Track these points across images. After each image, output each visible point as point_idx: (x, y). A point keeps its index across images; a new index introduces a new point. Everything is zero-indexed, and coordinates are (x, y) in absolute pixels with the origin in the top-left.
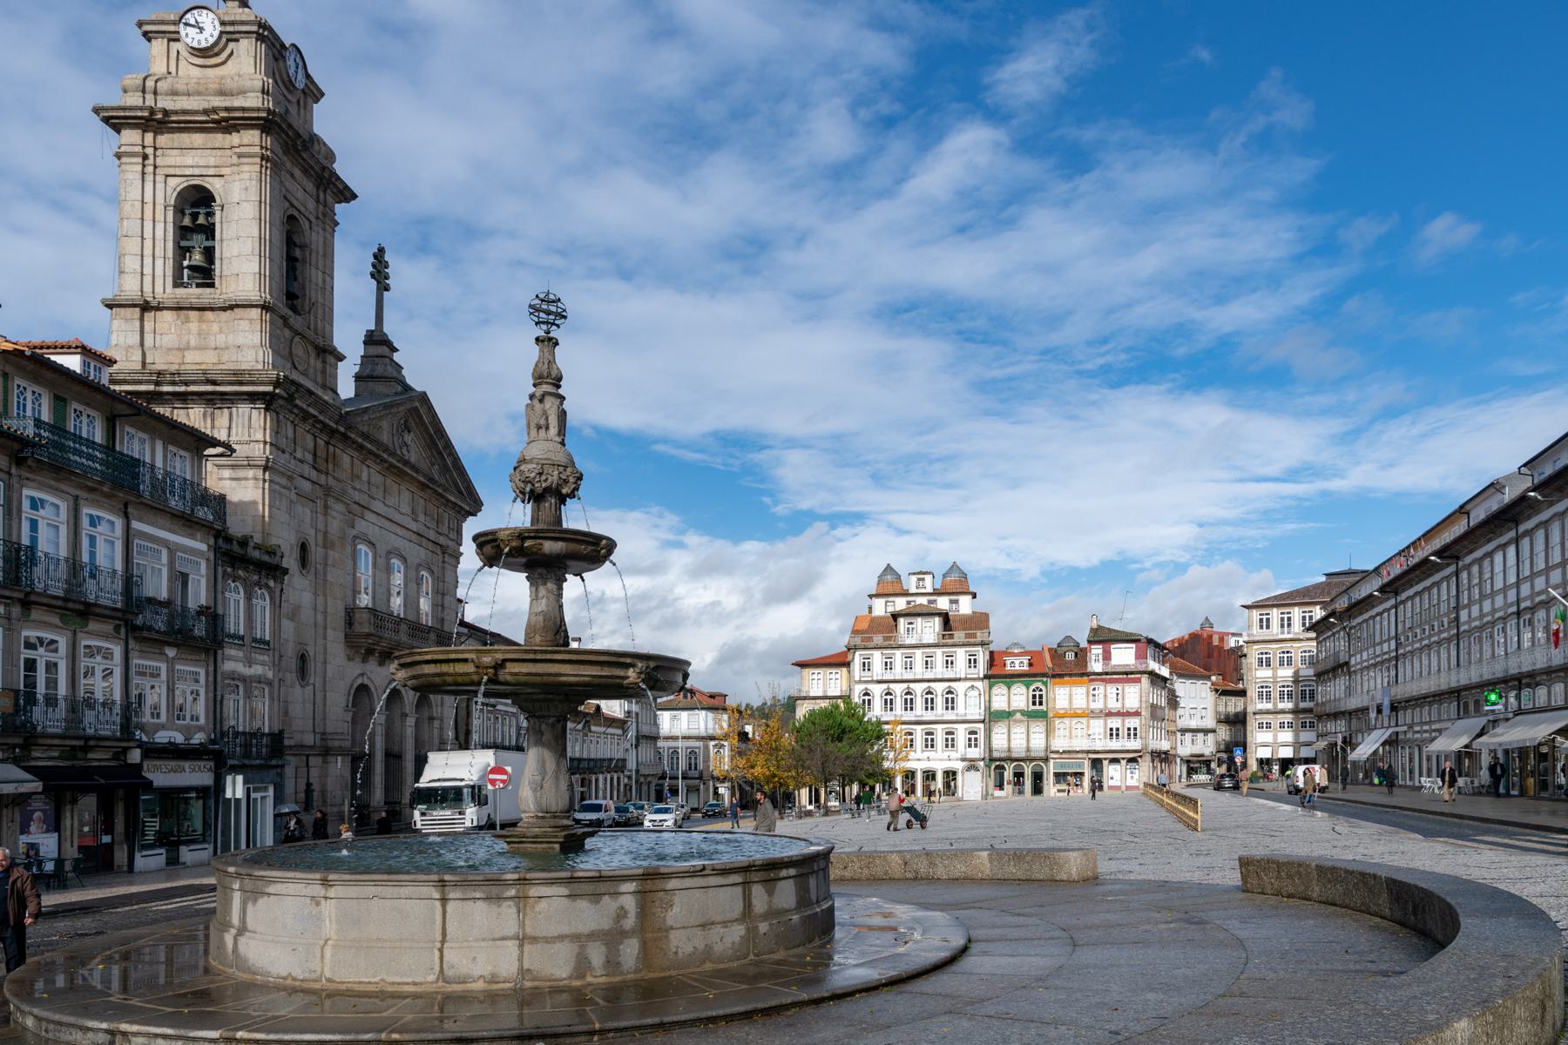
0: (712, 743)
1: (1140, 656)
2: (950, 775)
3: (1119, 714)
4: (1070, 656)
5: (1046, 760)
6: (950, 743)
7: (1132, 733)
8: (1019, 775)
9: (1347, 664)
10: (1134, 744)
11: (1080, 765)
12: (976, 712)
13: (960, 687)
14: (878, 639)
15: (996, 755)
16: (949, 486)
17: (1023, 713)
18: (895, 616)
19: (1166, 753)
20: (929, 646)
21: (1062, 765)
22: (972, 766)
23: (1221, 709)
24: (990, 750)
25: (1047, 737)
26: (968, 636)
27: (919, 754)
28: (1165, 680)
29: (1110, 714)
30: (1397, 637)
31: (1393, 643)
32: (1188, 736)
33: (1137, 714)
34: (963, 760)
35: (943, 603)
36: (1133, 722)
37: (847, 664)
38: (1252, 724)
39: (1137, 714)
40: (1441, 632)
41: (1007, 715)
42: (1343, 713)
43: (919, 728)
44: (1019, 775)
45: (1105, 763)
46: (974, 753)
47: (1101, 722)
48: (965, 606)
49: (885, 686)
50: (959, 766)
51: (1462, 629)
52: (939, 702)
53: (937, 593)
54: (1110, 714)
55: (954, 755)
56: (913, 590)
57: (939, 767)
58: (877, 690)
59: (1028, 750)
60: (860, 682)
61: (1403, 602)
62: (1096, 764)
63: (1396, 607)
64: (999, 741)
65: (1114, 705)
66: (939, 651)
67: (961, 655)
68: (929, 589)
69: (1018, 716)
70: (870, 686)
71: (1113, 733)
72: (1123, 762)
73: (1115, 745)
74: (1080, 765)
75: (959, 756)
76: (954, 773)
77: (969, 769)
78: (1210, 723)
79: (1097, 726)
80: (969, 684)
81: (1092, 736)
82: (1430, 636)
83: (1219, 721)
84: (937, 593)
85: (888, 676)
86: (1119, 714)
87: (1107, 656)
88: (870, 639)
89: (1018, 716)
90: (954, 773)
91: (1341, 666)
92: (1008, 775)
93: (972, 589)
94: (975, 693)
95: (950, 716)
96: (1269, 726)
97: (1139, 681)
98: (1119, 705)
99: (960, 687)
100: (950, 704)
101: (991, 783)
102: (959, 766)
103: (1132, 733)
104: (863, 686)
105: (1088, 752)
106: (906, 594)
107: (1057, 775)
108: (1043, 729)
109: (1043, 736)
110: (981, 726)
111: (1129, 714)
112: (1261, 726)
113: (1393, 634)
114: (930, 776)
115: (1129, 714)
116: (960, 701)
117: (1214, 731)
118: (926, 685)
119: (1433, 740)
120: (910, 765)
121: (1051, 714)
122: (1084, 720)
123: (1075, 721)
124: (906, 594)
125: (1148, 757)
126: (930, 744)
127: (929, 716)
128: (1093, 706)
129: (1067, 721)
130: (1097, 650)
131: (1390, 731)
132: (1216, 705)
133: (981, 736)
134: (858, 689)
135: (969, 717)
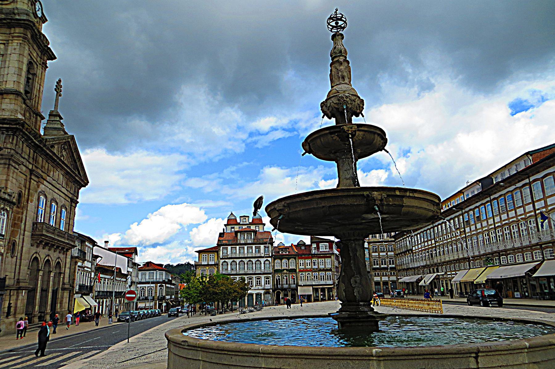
0: (159, 285)
1: (331, 247)
3: (323, 270)
9: (412, 250)
16: (257, 180)
17: (286, 270)
18: (236, 232)
20: (249, 244)
29: (321, 270)
30: (434, 239)
31: (433, 241)
33: (330, 270)
34: (263, 289)
35: (253, 227)
37: (217, 252)
39: (330, 270)
40: (456, 236)
41: (281, 271)
42: (411, 269)
46: (268, 286)
50: (262, 292)
51: (467, 235)
54: (321, 270)
55: (260, 287)
60: (222, 259)
61: (437, 226)
63: (433, 227)
65: (322, 267)
68: (247, 223)
69: (285, 271)
75: (262, 288)
80: (266, 259)
82: (451, 238)
84: (250, 224)
85: (234, 256)
86: (323, 270)
87: (318, 248)
89: (285, 271)
91: (408, 251)
97: (330, 257)
98: (323, 267)
99: (262, 260)
102: (262, 292)
104: (223, 260)
106: (239, 224)
110: (271, 276)
111: (327, 270)
113: (433, 237)
115: (327, 270)
119: (454, 277)
121: (298, 271)
130: (314, 245)
131: (435, 274)
134: (222, 261)
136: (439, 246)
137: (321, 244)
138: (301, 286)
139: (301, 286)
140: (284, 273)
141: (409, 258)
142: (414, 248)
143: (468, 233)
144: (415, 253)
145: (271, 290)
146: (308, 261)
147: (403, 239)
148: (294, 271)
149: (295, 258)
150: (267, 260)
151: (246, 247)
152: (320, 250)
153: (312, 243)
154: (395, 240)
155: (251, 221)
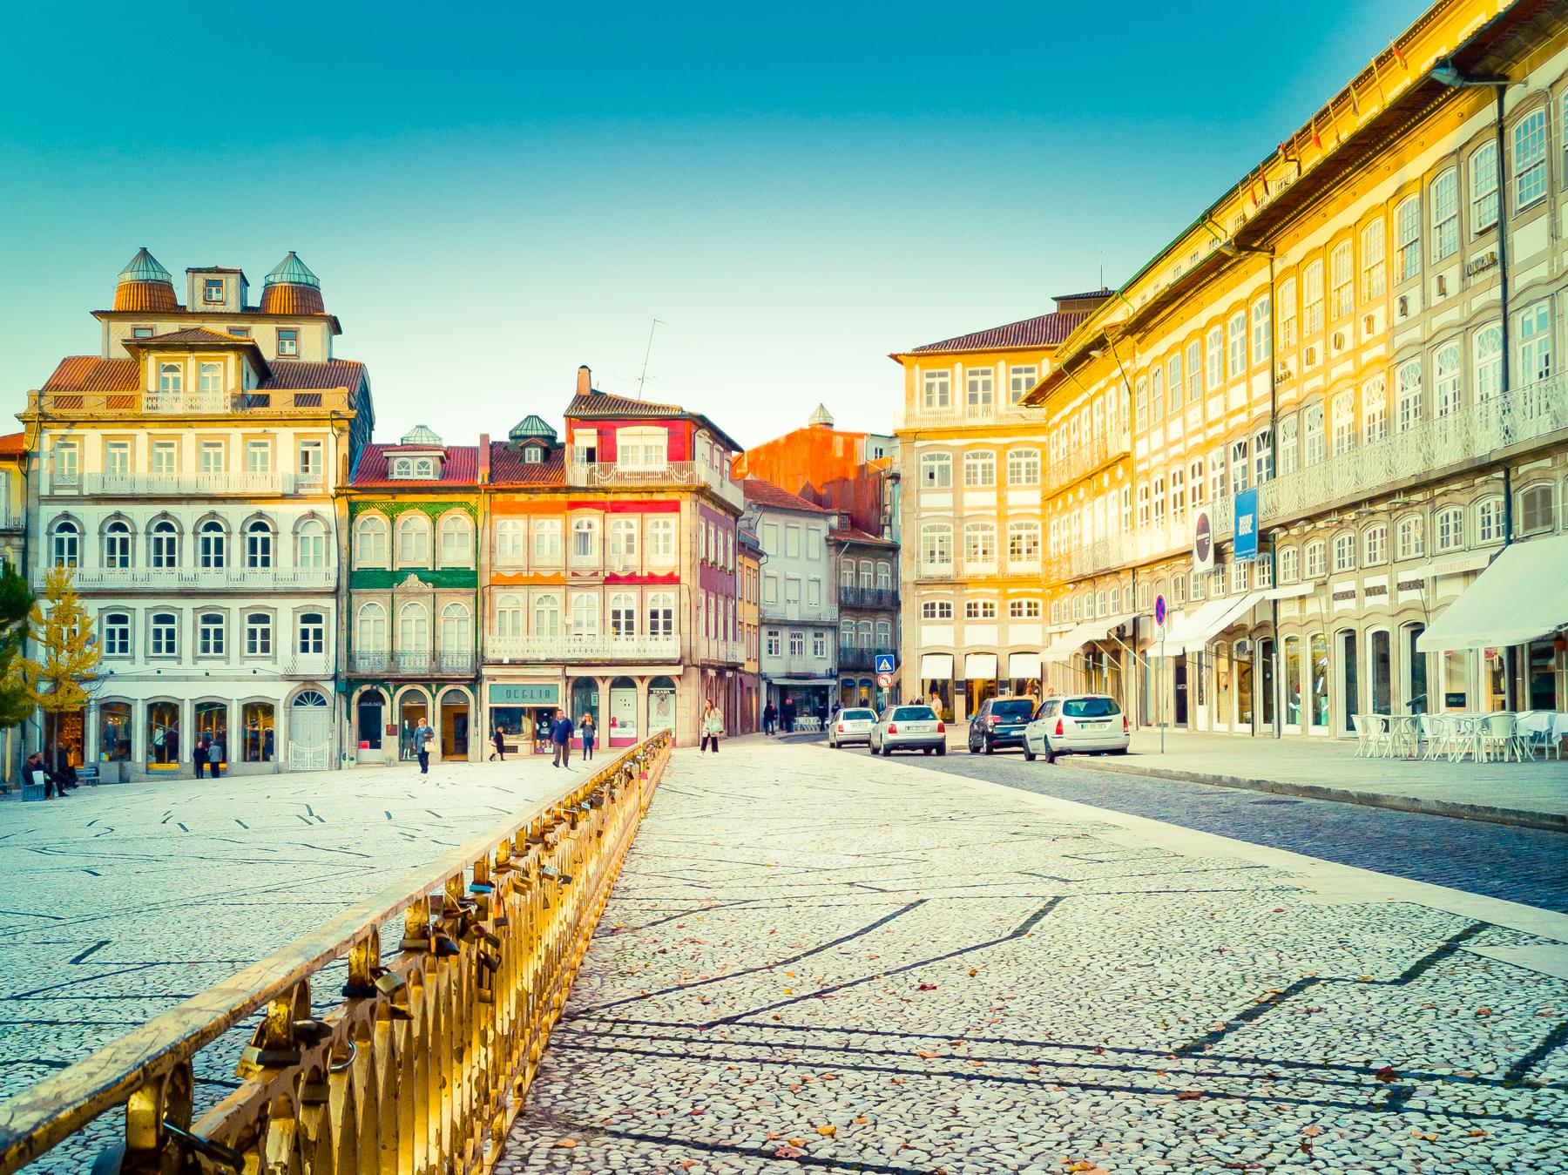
1: (680, 452)
2: (258, 710)
3: (631, 579)
4: (534, 455)
5: (475, 682)
6: (260, 641)
7: (660, 622)
8: (413, 714)
10: (667, 647)
11: (548, 692)
12: (323, 574)
13: (283, 515)
14: (94, 402)
15: (363, 668)
17: (422, 574)
19: (734, 667)
21: (509, 692)
22: (308, 696)
23: (847, 582)
24: (350, 658)
25: (477, 628)
26: (300, 401)
27: (187, 666)
28: (736, 513)
29: (612, 580)
32: (785, 637)
33: (672, 579)
36: (662, 598)
38: (911, 605)
39: (672, 579)
43: (188, 605)
44: (413, 714)
45: (604, 688)
47: (595, 595)
48: (311, 345)
49: (110, 509)
52: (236, 548)
53: (249, 313)
54: (612, 580)
55: (265, 666)
56: (200, 307)
57: (235, 694)
58: (92, 517)
59: (435, 656)
60: (51, 499)
62: (584, 686)
64: (371, 638)
66: (236, 433)
67: (286, 440)
68: (233, 307)
69: (413, 579)
70: (72, 509)
71: (622, 622)
72: (642, 688)
73: (624, 647)
74: (548, 692)
75: (279, 670)
76: (268, 710)
77: (301, 700)
78: (826, 610)
79: (588, 605)
80: (302, 509)
81: (575, 628)
83: (844, 608)
86: (631, 579)
88: (77, 402)
89: (413, 579)
90: (268, 710)
92: (389, 713)
93: (328, 311)
94: (316, 529)
95: (260, 578)
96: (946, 611)
97: (674, 507)
100: (259, 552)
101: (351, 730)
102: (279, 693)
103: (660, 622)
104: (59, 509)
105: (565, 664)
106: (179, 312)
107: (497, 713)
108: (470, 611)
109: (469, 627)
110: (330, 603)
111: (652, 580)
112: (929, 610)
114: (212, 713)
115: (652, 580)
116: (283, 550)
117: (833, 627)
118: (203, 509)
120: (110, 690)
121: (485, 580)
122: (557, 593)
123: (538, 593)
124: (179, 312)
125: (695, 675)
126: (213, 643)
127: (211, 578)
128: (577, 561)
129: (519, 595)
130: (587, 438)
132: (837, 571)
133: (329, 627)
135: (304, 584)
136: (1299, 407)
137: (625, 437)
138: (499, 663)
139: (499, 663)
140: (407, 594)
141: (1113, 512)
142: (1141, 450)
143: (1531, 263)
144: (1147, 474)
145: (330, 687)
146: (550, 528)
147: (1091, 400)
148: (462, 579)
149: (472, 511)
150: (313, 515)
151: (189, 435)
152: (620, 466)
153: (573, 421)
154: (1048, 418)
155: (254, 300)
